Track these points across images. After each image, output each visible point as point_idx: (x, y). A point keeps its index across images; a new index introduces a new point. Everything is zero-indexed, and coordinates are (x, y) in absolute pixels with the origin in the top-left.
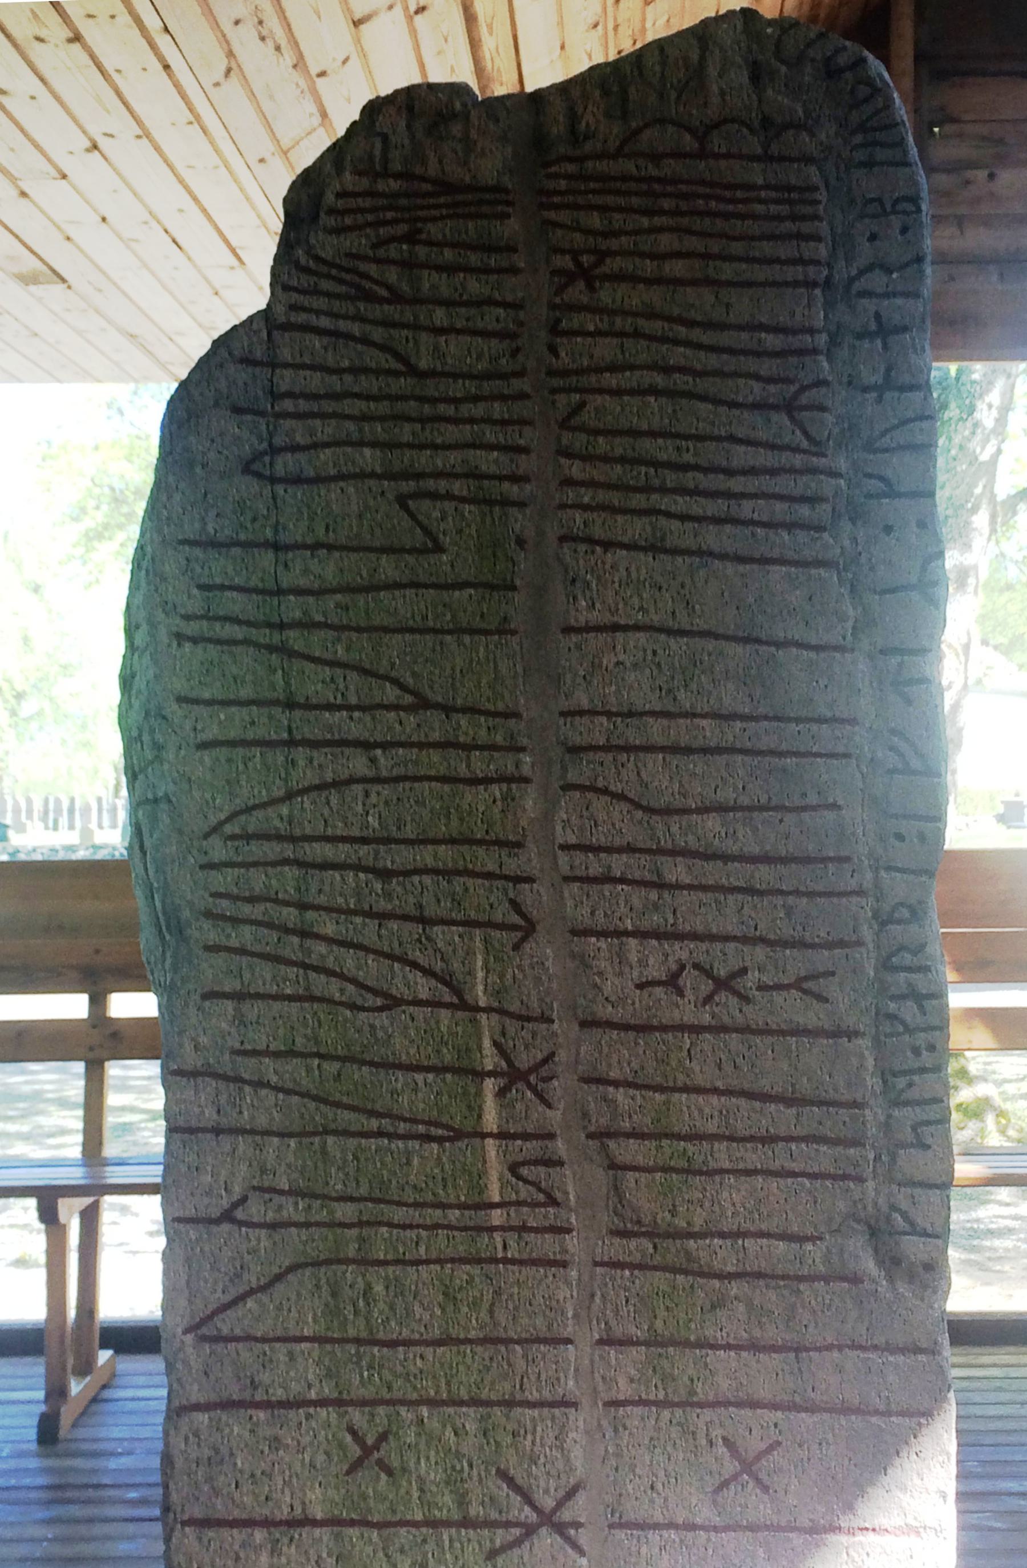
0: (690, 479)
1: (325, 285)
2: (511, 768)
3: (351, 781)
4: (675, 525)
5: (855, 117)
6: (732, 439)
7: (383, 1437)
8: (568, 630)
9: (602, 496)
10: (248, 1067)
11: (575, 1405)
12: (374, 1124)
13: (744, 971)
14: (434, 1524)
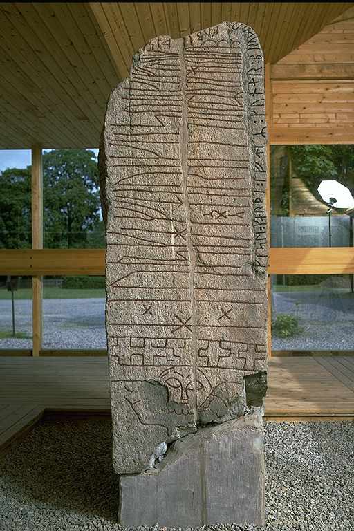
0: (215, 112)
1: (141, 73)
2: (177, 171)
3: (145, 173)
4: (212, 121)
5: (249, 40)
6: (223, 103)
7: (150, 307)
8: (189, 142)
9: (197, 115)
10: (123, 231)
11: (190, 301)
12: (149, 243)
13: (225, 212)
14: (161, 325)
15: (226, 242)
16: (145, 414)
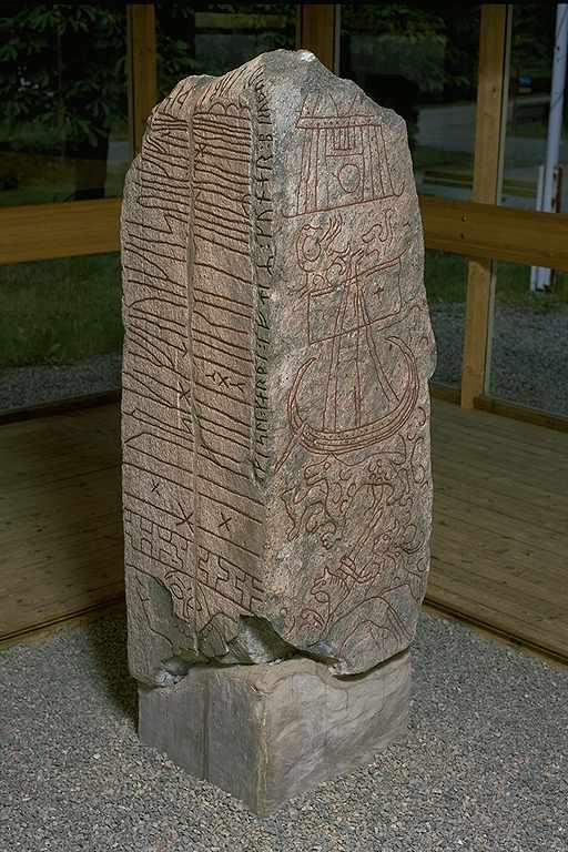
15: (228, 422)
16: (153, 617)
